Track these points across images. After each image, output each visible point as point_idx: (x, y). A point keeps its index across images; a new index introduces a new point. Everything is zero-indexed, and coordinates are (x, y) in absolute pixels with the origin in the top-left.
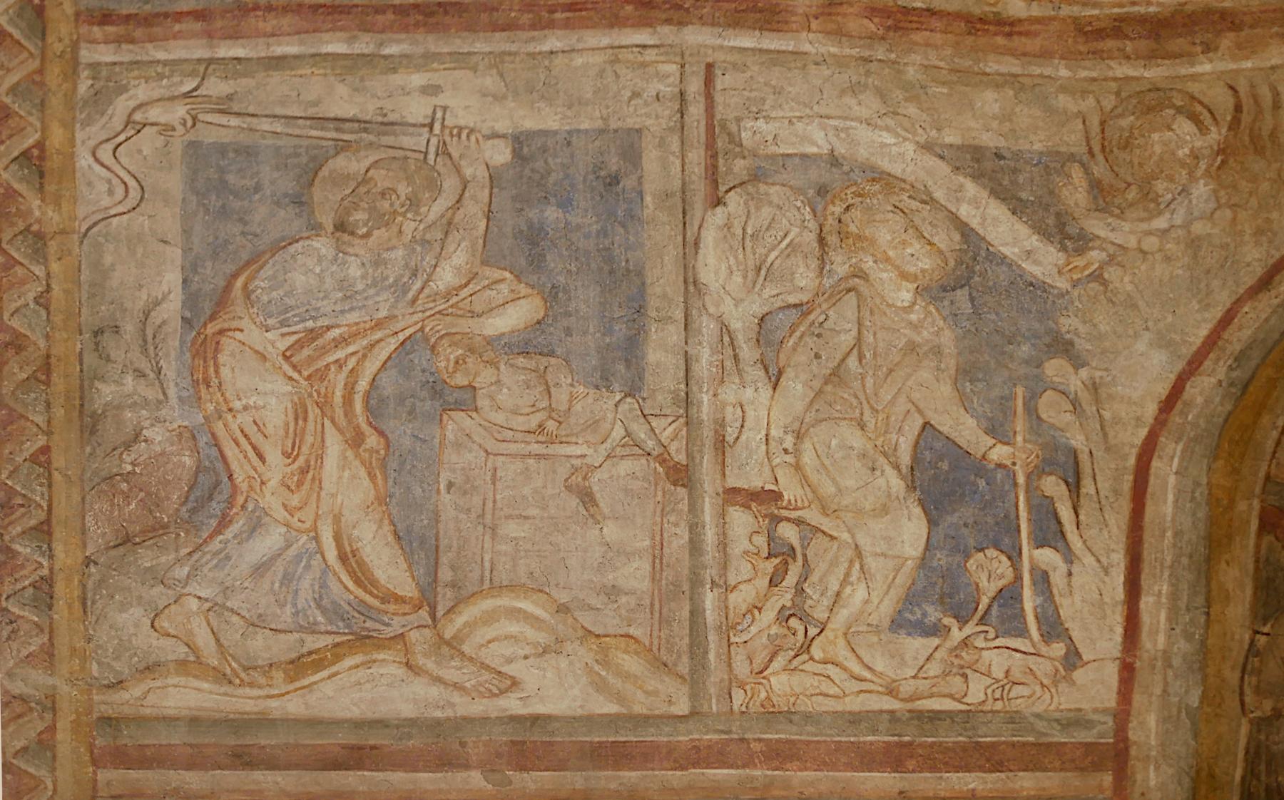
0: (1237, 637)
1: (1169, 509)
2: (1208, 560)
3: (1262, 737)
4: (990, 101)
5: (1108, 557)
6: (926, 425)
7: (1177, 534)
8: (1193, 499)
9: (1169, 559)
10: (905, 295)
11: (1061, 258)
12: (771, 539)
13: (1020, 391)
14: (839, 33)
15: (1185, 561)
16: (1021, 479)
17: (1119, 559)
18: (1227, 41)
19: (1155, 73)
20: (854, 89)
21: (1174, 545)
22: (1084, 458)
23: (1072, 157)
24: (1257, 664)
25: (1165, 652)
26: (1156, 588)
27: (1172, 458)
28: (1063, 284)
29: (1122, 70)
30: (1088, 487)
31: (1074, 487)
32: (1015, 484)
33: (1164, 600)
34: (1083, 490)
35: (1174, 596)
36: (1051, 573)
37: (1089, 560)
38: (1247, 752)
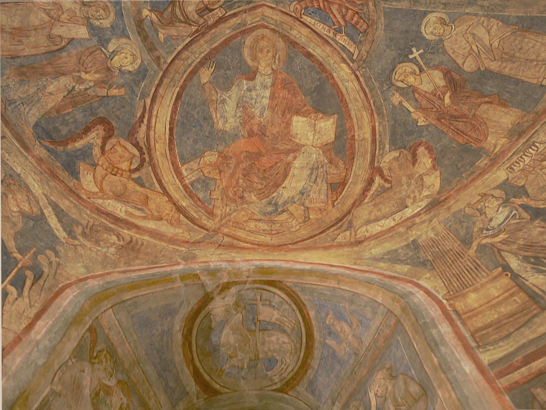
0: (65, 354)
1: (65, 303)
2: (71, 323)
3: (51, 399)
5: (34, 303)
7: (64, 311)
8: (75, 305)
9: (57, 315)
15: (63, 319)
16: (20, 265)
17: (38, 306)
21: (61, 313)
22: (45, 276)
24: (65, 369)
25: (38, 341)
26: (47, 321)
27: (75, 292)
30: (41, 282)
31: (37, 279)
32: (16, 265)
33: (48, 326)
34: (39, 282)
35: (52, 327)
36: (9, 295)
37: (27, 300)
38: (43, 400)
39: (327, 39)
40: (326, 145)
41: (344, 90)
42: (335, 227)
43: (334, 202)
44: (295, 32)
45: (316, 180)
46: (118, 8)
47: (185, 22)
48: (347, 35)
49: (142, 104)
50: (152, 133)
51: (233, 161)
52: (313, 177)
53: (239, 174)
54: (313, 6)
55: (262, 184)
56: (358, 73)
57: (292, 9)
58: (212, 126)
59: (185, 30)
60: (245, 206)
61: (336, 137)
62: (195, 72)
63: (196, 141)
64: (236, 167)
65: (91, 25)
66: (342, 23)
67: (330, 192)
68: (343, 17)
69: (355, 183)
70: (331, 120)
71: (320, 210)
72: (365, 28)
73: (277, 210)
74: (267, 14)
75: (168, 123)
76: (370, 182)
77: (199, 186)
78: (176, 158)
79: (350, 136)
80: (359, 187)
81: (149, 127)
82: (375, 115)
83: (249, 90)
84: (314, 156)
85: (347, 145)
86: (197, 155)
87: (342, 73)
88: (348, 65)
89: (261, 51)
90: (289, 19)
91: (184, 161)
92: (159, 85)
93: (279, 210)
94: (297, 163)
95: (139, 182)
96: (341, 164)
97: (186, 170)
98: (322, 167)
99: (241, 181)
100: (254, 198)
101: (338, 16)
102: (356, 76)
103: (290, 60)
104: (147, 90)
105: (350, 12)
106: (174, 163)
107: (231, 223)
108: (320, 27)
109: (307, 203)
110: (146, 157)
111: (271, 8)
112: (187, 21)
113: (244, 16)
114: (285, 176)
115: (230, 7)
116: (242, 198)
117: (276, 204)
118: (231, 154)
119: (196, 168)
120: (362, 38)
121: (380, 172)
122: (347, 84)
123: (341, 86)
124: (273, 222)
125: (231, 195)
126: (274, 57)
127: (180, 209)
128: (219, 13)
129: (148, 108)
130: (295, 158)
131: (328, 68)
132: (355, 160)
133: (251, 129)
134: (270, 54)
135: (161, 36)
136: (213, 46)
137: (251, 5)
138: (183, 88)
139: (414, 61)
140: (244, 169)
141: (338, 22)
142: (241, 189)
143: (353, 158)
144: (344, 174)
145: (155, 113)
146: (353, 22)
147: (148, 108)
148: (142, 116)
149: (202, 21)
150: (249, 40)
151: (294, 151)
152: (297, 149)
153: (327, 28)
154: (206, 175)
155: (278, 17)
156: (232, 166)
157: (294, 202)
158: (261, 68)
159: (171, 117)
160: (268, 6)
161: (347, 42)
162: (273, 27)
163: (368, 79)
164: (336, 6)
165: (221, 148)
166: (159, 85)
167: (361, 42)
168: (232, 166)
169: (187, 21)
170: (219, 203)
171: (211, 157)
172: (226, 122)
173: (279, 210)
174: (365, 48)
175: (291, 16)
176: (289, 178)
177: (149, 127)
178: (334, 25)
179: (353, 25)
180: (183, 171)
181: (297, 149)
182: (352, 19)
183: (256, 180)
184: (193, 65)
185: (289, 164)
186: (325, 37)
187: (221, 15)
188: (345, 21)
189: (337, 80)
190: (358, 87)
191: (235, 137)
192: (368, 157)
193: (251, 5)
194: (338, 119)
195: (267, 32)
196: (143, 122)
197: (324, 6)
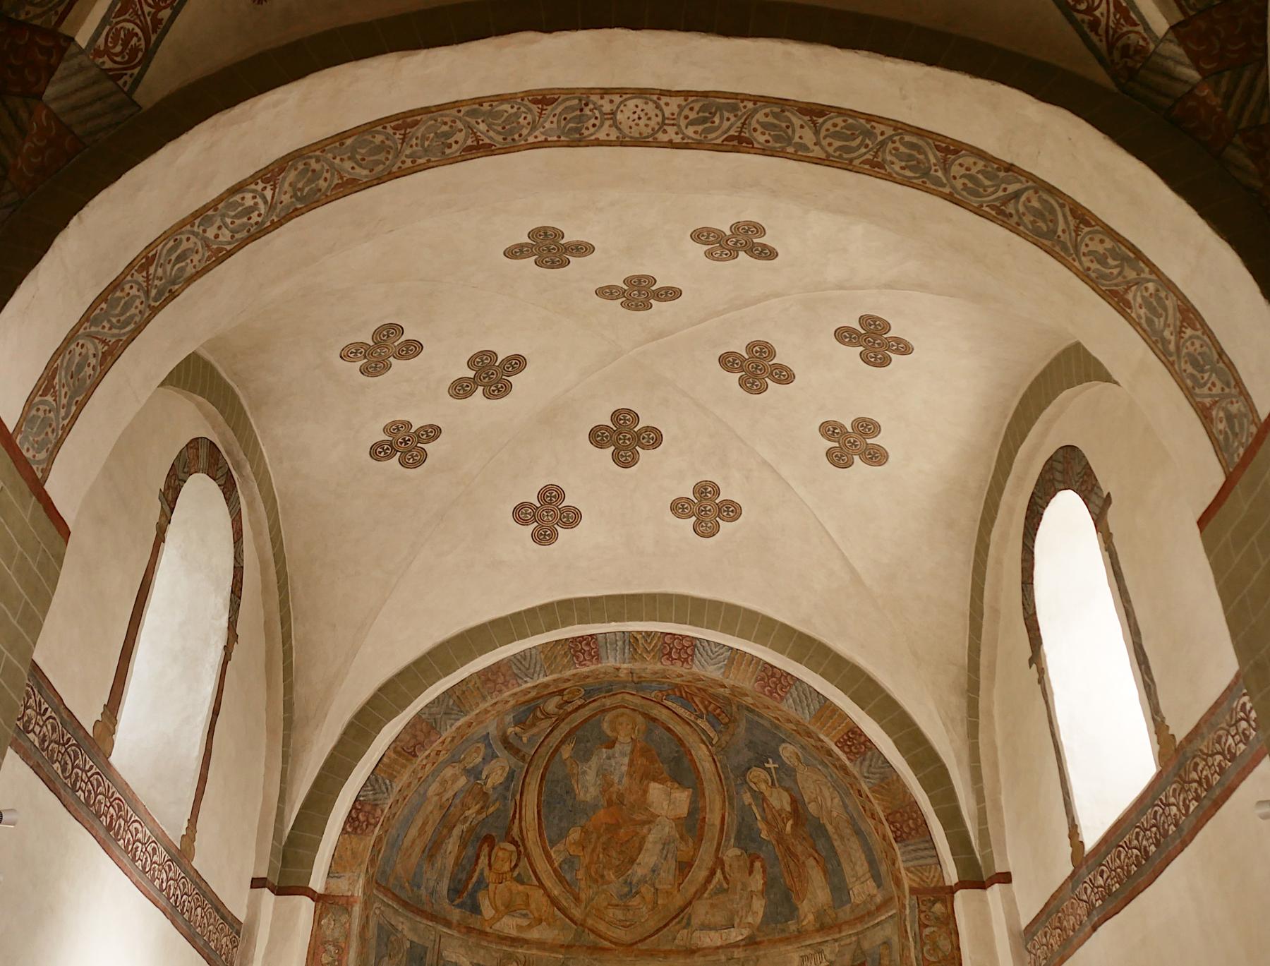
4: (482, 952)
14: (459, 932)
18: (526, 946)
19: (511, 950)
20: (461, 946)
29: (505, 948)
40: (679, 818)
41: (701, 769)
42: (677, 920)
43: (680, 884)
44: (655, 712)
45: (666, 856)
46: (487, 742)
47: (546, 718)
49: (513, 804)
50: (523, 823)
51: (594, 836)
52: (665, 852)
53: (599, 849)
54: (675, 694)
55: (619, 860)
56: (715, 757)
58: (575, 798)
60: (605, 887)
61: (689, 813)
62: (557, 749)
63: (561, 820)
64: (596, 843)
66: (704, 712)
67: (677, 872)
68: (706, 708)
69: (699, 868)
70: (686, 793)
71: (667, 892)
73: (631, 890)
76: (713, 873)
77: (566, 867)
78: (545, 843)
79: (701, 817)
80: (704, 874)
82: (727, 803)
83: (609, 758)
84: (667, 829)
85: (698, 826)
86: (563, 835)
87: (700, 752)
89: (621, 724)
91: (553, 844)
92: (525, 777)
93: (634, 891)
94: (651, 838)
95: (520, 880)
96: (691, 843)
97: (555, 852)
98: (673, 842)
99: (601, 856)
100: (613, 877)
101: (701, 706)
102: (714, 759)
103: (649, 732)
105: (712, 705)
106: (544, 848)
107: (594, 911)
109: (657, 886)
110: (522, 849)
111: (632, 694)
113: (603, 700)
114: (640, 849)
115: (590, 697)
116: (602, 876)
117: (631, 883)
118: (591, 829)
119: (562, 849)
122: (703, 763)
123: (698, 764)
124: (627, 908)
125: (593, 874)
126: (633, 729)
127: (554, 902)
128: (579, 703)
129: (518, 803)
131: (687, 744)
132: (703, 842)
133: (610, 798)
134: (630, 727)
135: (525, 739)
136: (573, 725)
138: (546, 768)
139: (768, 770)
140: (603, 844)
141: (700, 710)
142: (602, 866)
143: (702, 840)
144: (692, 853)
145: (524, 804)
147: (518, 803)
148: (515, 812)
149: (561, 711)
150: (608, 717)
151: (649, 822)
152: (651, 820)
155: (637, 701)
156: (593, 840)
157: (646, 882)
158: (621, 739)
163: (724, 767)
165: (583, 822)
166: (525, 777)
167: (721, 732)
168: (593, 840)
170: (583, 884)
171: (575, 835)
172: (587, 792)
173: (634, 891)
174: (725, 738)
176: (643, 852)
178: (696, 711)
180: (552, 854)
181: (651, 820)
183: (614, 854)
184: (555, 745)
185: (644, 839)
189: (695, 757)
190: (714, 769)
191: (595, 807)
192: (715, 843)
194: (693, 793)
195: (627, 711)
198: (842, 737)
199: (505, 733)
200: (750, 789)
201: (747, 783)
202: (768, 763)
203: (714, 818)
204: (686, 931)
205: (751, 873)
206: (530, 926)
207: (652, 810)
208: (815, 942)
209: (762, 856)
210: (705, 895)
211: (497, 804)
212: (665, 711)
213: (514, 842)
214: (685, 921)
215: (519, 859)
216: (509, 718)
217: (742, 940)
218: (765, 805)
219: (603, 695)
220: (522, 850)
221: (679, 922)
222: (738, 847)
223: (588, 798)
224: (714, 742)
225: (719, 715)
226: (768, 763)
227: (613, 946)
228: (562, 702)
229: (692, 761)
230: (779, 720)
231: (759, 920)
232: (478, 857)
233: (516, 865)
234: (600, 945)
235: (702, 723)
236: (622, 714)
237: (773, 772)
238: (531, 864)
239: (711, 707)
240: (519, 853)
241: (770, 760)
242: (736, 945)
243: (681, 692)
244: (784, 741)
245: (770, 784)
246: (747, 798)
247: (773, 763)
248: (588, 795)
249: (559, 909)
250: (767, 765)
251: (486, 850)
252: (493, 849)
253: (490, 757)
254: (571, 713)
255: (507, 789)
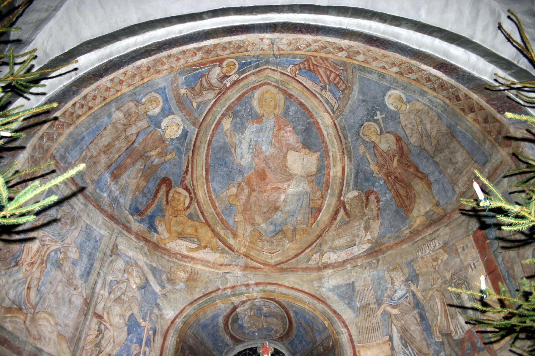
6: (132, 314)
10: (134, 287)
11: (160, 289)
12: (99, 327)
13: (149, 312)
23: (165, 272)
28: (159, 293)
39: (315, 93)
42: (310, 249)
43: (312, 224)
48: (331, 92)
49: (187, 159)
54: (305, 68)
57: (289, 71)
59: (210, 96)
62: (219, 123)
65: (149, 115)
68: (328, 77)
72: (344, 87)
74: (270, 75)
75: (204, 165)
76: (337, 212)
81: (192, 172)
82: (346, 158)
88: (330, 114)
90: (285, 77)
93: (277, 229)
95: (191, 217)
104: (189, 147)
108: (309, 84)
112: (211, 88)
115: (243, 73)
120: (341, 96)
121: (343, 204)
128: (235, 78)
129: (190, 159)
130: (289, 186)
135: (195, 105)
137: (258, 69)
139: (376, 121)
145: (195, 161)
146: (335, 82)
147: (190, 159)
148: (188, 167)
150: (257, 94)
153: (316, 85)
154: (231, 203)
159: (206, 160)
160: (271, 69)
161: (330, 97)
162: (274, 84)
164: (323, 70)
167: (340, 98)
169: (211, 88)
175: (288, 76)
177: (192, 172)
178: (321, 82)
179: (335, 84)
182: (335, 80)
186: (314, 92)
187: (236, 79)
188: (329, 81)
189: (322, 126)
193: (258, 69)
194: (320, 156)
196: (188, 170)
197: (314, 68)
198: (438, 65)
199: (178, 93)
200: (364, 141)
201: (361, 137)
202: (376, 115)
203: (335, 171)
204: (318, 254)
205: (367, 205)
206: (196, 249)
207: (291, 172)
208: (427, 234)
209: (375, 190)
210: (332, 228)
211: (174, 154)
212: (297, 85)
213: (186, 189)
214: (317, 249)
215: (191, 203)
216: (181, 80)
217: (364, 252)
218: (376, 151)
219: (253, 71)
220: (194, 197)
221: (312, 250)
222: (356, 190)
223: (243, 163)
224: (335, 109)
225: (338, 83)
226: (376, 115)
227: (262, 266)
228: (222, 75)
229: (319, 129)
230: (384, 68)
231: (376, 235)
232: (157, 191)
233: (188, 207)
234: (252, 265)
235: (328, 95)
236: (268, 91)
237: (381, 121)
238: (200, 208)
239: (331, 78)
240: (191, 199)
241: (378, 113)
242: (358, 257)
243: (309, 66)
244: (389, 89)
245: (379, 131)
246: (362, 149)
247: (381, 115)
248: (243, 160)
249: (219, 239)
250: (375, 118)
251: (163, 189)
252: (170, 189)
253: (166, 112)
254: (228, 89)
255: (182, 144)
